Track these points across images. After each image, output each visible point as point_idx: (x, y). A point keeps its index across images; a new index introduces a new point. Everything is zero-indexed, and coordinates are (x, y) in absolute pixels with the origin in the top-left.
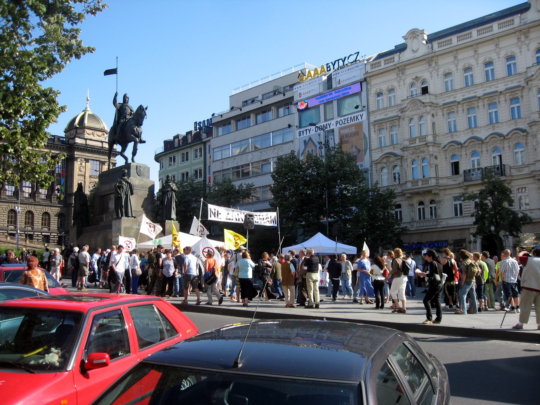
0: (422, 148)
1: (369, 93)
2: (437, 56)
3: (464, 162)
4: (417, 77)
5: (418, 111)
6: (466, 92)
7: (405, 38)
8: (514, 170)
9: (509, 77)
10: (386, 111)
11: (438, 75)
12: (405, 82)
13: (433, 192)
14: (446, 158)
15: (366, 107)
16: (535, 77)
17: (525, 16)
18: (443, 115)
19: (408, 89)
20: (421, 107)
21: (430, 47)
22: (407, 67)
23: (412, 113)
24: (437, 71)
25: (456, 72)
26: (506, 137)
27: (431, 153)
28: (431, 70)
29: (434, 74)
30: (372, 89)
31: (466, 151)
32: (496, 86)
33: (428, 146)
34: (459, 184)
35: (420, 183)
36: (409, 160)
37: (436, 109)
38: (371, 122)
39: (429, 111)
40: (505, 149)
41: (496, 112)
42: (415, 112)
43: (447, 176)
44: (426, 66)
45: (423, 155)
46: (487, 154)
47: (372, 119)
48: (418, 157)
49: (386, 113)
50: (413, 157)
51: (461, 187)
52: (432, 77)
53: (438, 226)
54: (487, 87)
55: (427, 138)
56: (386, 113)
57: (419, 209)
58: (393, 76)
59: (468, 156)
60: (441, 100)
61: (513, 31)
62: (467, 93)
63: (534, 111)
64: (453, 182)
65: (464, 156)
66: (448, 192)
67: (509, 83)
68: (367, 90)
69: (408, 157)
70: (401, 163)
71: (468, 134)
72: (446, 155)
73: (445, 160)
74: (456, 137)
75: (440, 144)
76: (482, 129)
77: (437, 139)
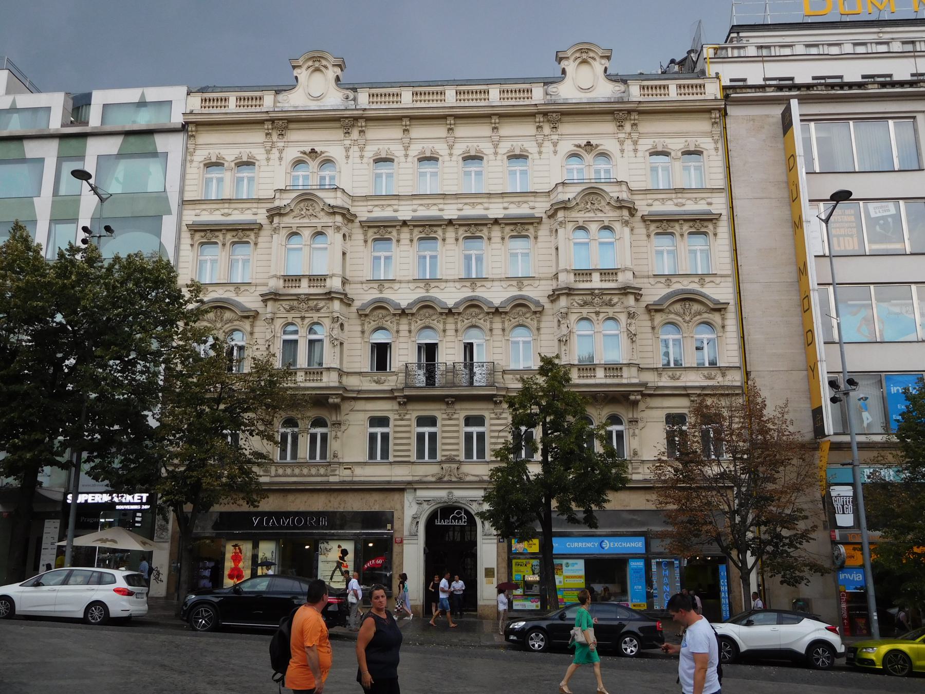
0: (315, 302)
1: (189, 158)
3: (402, 346)
6: (421, 205)
8: (511, 376)
11: (362, 157)
12: (284, 155)
13: (331, 400)
14: (363, 332)
17: (554, 90)
18: (366, 241)
20: (322, 213)
22: (291, 126)
23: (297, 220)
24: (362, 150)
26: (501, 310)
27: (335, 315)
29: (355, 152)
30: (198, 152)
31: (410, 324)
32: (486, 205)
33: (332, 299)
34: (392, 391)
35: (300, 377)
37: (350, 224)
38: (184, 223)
39: (340, 225)
42: (306, 220)
43: (362, 370)
47: (190, 216)
48: (303, 318)
49: (226, 211)
51: (395, 398)
52: (347, 157)
53: (332, 479)
54: (466, 204)
55: (328, 280)
57: (421, 437)
58: (257, 136)
60: (365, 209)
61: (533, 110)
62: (423, 208)
63: (568, 268)
64: (374, 384)
66: (360, 405)
69: (278, 316)
70: (252, 326)
72: (363, 325)
73: (359, 334)
74: (389, 291)
75: (353, 300)
76: (449, 284)
77: (347, 287)
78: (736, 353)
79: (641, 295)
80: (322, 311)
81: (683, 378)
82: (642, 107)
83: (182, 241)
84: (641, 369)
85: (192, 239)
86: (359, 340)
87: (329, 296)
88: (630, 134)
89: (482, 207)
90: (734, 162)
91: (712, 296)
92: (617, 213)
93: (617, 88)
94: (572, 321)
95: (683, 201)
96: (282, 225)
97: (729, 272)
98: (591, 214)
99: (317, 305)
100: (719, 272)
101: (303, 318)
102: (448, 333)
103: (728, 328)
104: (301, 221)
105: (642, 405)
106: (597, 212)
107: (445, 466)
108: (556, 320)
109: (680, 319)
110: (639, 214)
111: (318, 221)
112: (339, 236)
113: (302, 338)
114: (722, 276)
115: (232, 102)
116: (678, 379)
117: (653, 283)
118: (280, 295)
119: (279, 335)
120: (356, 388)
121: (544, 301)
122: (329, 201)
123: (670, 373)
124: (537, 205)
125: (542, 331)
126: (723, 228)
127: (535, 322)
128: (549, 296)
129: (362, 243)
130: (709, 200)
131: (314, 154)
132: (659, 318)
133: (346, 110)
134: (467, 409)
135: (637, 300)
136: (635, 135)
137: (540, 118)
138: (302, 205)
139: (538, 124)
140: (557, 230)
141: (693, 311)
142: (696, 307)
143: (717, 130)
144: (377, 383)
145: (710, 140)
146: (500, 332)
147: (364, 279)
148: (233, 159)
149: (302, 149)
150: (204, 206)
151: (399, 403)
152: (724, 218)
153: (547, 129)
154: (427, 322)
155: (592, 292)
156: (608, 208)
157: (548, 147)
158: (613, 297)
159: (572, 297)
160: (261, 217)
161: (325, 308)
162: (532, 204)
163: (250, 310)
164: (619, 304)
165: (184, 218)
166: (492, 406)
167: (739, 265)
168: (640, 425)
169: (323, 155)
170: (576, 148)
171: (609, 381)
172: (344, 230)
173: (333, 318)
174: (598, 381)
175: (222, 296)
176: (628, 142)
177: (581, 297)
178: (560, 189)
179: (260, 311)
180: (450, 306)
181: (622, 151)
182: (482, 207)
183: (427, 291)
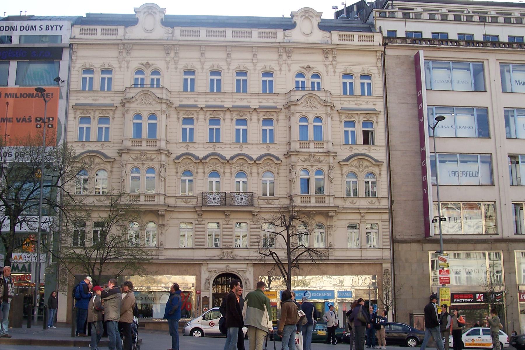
1: (73, 65)
2: (180, 45)
4: (148, 63)
5: (149, 106)
6: (211, 98)
7: (136, 10)
8: (262, 201)
9: (184, 93)
10: (96, 94)
11: (176, 68)
12: (130, 65)
13: (160, 213)
14: (177, 173)
15: (66, 83)
16: (300, 102)
17: (289, 34)
19: (132, 75)
21: (170, 32)
22: (135, 47)
23: (139, 106)
25: (200, 71)
27: (163, 163)
28: (168, 59)
29: (172, 65)
30: (78, 62)
31: (204, 169)
36: (129, 167)
38: (71, 105)
39: (165, 109)
40: (253, 175)
41: (87, 128)
42: (145, 106)
44: (162, 54)
45: (151, 163)
46: (231, 176)
47: (73, 101)
48: (143, 164)
49: (95, 98)
50: (136, 163)
52: (168, 68)
53: (160, 257)
55: (158, 142)
56: (95, 98)
58: (113, 53)
59: (206, 175)
60: (178, 99)
63: (296, 140)
64: (184, 203)
65: (200, 174)
67: (264, 101)
68: (71, 60)
69: (129, 162)
70: (112, 167)
71: (209, 149)
74: (192, 149)
77: (168, 145)
78: (386, 190)
79: (336, 156)
80: (154, 160)
81: (357, 203)
82: (339, 47)
83: (70, 115)
84: (335, 198)
85: (75, 114)
86: (175, 177)
87: (159, 151)
88: (332, 62)
89: (247, 101)
90: (389, 81)
91: (374, 157)
92: (324, 108)
93: (326, 35)
94: (298, 170)
95: (361, 102)
96: (131, 109)
97: (384, 144)
98: (310, 109)
99: (151, 156)
100: (378, 144)
101: (143, 164)
102: (226, 174)
103: (383, 176)
104: (142, 106)
105: (335, 219)
106: (313, 108)
107: (224, 251)
108: (288, 169)
109: (357, 170)
110: (336, 109)
111: (151, 107)
112: (164, 116)
113: (142, 176)
114: (380, 146)
115: (99, 31)
116: (355, 204)
117: (342, 149)
118: (130, 150)
119: (129, 174)
120: (173, 205)
121: (281, 157)
122: (159, 95)
123: (351, 201)
124: (278, 101)
125: (280, 175)
126: (381, 119)
127: (276, 170)
128: (284, 155)
129: (176, 120)
130: (375, 103)
131: (148, 65)
132: (346, 169)
133: (167, 40)
134: (237, 219)
135: (334, 158)
136: (334, 63)
137: (281, 50)
138: (142, 97)
139: (280, 54)
140: (290, 117)
141: (364, 166)
142: (366, 163)
143: (380, 64)
144: (185, 202)
145: (376, 68)
146: (256, 175)
147: (178, 141)
148: (99, 66)
149: (140, 62)
150: (82, 95)
151: (198, 215)
152: (382, 113)
153: (284, 57)
154: (215, 168)
155: (310, 154)
156: (319, 106)
157: (285, 67)
158: (321, 157)
159: (298, 156)
160: (117, 103)
161: (156, 159)
162: (275, 101)
163: (110, 158)
164: (324, 161)
165: (70, 101)
166: (251, 217)
167: (390, 140)
168: (334, 229)
169: (153, 66)
170: (301, 69)
171: (318, 205)
172: (167, 112)
173: (161, 165)
174: (312, 205)
175: (94, 149)
176: (331, 67)
177: (303, 157)
178: (292, 93)
179: (116, 158)
180: (228, 159)
181: (327, 72)
182: (247, 101)
183: (214, 150)
